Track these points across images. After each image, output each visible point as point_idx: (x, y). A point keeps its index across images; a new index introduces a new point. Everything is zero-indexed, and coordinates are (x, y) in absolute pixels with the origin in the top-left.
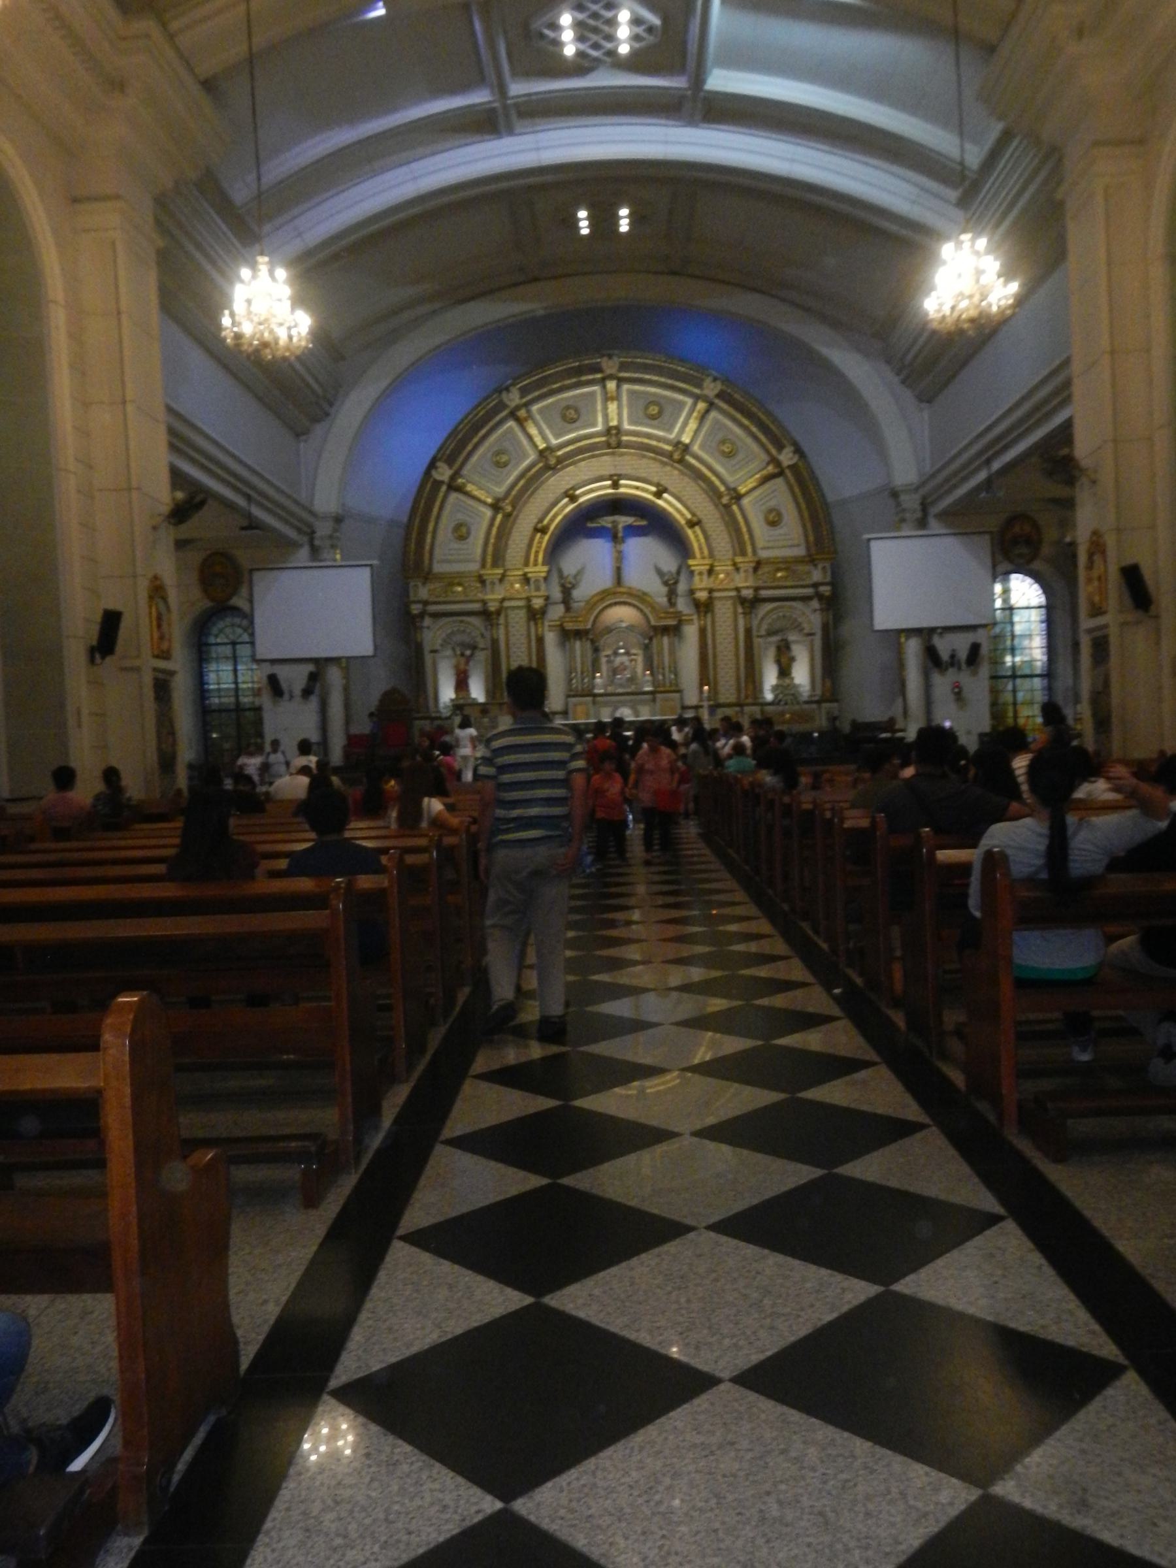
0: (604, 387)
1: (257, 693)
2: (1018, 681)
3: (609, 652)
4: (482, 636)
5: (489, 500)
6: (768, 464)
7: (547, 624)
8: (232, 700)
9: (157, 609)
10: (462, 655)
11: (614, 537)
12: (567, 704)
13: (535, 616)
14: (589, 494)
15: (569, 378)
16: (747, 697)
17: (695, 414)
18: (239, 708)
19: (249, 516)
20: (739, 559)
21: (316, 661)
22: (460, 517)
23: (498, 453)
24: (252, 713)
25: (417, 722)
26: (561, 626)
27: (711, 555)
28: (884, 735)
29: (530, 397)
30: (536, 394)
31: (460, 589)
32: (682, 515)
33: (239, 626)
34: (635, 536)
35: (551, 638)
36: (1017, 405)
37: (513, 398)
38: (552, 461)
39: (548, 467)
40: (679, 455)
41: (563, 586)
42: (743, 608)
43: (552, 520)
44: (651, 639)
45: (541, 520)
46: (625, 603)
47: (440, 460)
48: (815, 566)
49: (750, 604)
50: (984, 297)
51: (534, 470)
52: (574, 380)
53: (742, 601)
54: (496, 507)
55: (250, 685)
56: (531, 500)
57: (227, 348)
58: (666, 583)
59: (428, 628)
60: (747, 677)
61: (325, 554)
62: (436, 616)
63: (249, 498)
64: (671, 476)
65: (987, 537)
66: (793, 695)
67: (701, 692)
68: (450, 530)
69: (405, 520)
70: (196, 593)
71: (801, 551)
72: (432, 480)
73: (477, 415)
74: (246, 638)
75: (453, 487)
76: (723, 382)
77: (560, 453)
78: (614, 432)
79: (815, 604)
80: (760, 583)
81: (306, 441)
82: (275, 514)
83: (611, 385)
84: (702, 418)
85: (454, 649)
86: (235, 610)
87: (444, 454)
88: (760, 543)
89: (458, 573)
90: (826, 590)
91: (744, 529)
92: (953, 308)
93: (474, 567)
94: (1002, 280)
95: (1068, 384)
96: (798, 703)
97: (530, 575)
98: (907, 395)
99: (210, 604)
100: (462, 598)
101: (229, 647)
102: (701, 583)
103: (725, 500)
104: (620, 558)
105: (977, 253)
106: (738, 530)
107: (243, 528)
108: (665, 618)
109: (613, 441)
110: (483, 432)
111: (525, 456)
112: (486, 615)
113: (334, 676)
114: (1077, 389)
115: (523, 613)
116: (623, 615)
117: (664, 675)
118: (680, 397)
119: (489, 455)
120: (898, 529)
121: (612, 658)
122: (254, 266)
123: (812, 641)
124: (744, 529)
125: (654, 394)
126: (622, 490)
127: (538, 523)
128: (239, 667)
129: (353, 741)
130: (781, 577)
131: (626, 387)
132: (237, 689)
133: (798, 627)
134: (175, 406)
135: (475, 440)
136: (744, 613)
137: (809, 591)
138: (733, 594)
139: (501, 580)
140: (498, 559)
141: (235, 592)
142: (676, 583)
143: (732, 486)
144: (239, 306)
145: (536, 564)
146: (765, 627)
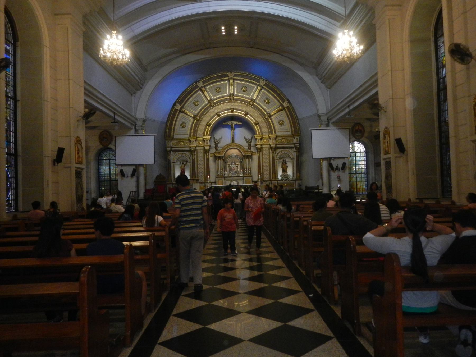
0: (229, 82)
1: (116, 175)
2: (357, 174)
3: (230, 164)
4: (189, 158)
6: (280, 106)
7: (210, 154)
8: (109, 177)
9: (78, 147)
11: (232, 128)
12: (216, 179)
13: (206, 152)
14: (224, 114)
15: (219, 79)
16: (273, 178)
17: (257, 90)
18: (110, 180)
19: (115, 119)
20: (270, 135)
21: (136, 165)
22: (183, 120)
23: (195, 101)
24: (115, 182)
25: (168, 185)
26: (214, 155)
27: (262, 134)
28: (315, 191)
29: (206, 84)
30: (208, 83)
31: (183, 143)
32: (253, 121)
33: (112, 154)
34: (239, 128)
35: (211, 159)
36: (358, 88)
37: (201, 84)
38: (212, 104)
39: (211, 106)
40: (252, 103)
41: (215, 142)
42: (272, 150)
43: (212, 122)
44: (243, 160)
45: (208, 122)
46: (234, 148)
47: (177, 103)
48: (295, 138)
49: (274, 149)
50: (352, 50)
51: (207, 106)
52: (220, 79)
53: (271, 148)
54: (194, 118)
55: (115, 173)
56: (206, 116)
57: (101, 61)
58: (248, 142)
59: (172, 155)
60: (272, 172)
61: (140, 132)
63: (114, 113)
64: (249, 109)
65: (348, 130)
66: (287, 178)
67: (258, 176)
68: (180, 125)
69: (166, 121)
70: (98, 143)
71: (290, 133)
73: (189, 89)
74: (114, 158)
75: (181, 111)
76: (266, 82)
77: (214, 101)
78: (232, 95)
79: (294, 149)
80: (277, 143)
81: (134, 96)
82: (123, 119)
83: (231, 81)
84: (259, 92)
85: (180, 162)
86: (110, 149)
88: (277, 131)
90: (297, 145)
91: (272, 126)
92: (342, 53)
93: (187, 136)
94: (358, 44)
95: (377, 80)
96: (289, 180)
97: (204, 139)
98: (323, 86)
99: (101, 146)
100: (184, 146)
101: (108, 160)
102: (259, 143)
103: (266, 117)
104: (233, 134)
105: (350, 37)
106: (270, 126)
107: (112, 123)
108: (247, 153)
109: (232, 98)
111: (204, 102)
112: (190, 151)
113: (142, 170)
114: (379, 82)
115: (202, 151)
116: (234, 152)
117: (247, 171)
118: (253, 85)
119: (193, 102)
120: (321, 127)
122: (111, 35)
123: (293, 161)
124: (272, 126)
125: (245, 84)
126: (234, 113)
128: (111, 167)
129: (147, 191)
130: (284, 141)
131: (236, 82)
132: (110, 174)
133: (289, 157)
134: (86, 81)
135: (188, 97)
136: (272, 152)
137: (293, 145)
138: (269, 146)
139: (195, 141)
140: (195, 133)
141: (110, 143)
142: (251, 142)
143: (268, 113)
144: (105, 47)
145: (207, 135)
146: (278, 156)
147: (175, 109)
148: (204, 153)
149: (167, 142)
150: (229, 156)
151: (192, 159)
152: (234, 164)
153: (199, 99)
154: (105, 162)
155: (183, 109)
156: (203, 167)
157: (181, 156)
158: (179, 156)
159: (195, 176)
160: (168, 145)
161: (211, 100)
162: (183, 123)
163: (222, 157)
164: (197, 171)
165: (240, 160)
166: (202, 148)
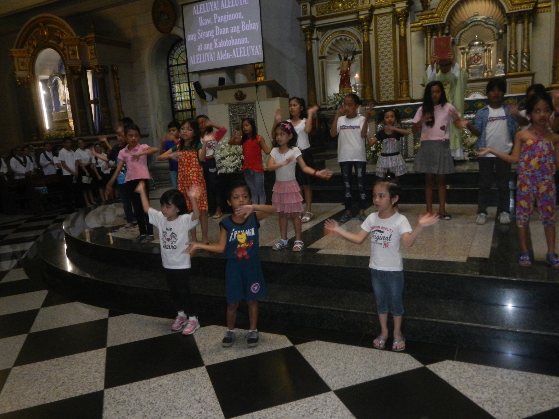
4: (359, 42)
7: (409, 25)
10: (346, 59)
31: (340, 5)
35: (413, 37)
59: (317, 39)
62: (324, 29)
112: (357, 23)
115: (389, 19)
117: (516, 62)
121: (467, 50)
141: (174, 24)
148: (394, 24)
149: (301, 4)
150: (464, 22)
151: (364, 42)
152: (479, 45)
154: (180, 69)
157: (338, 38)
158: (334, 41)
159: (372, 86)
160: (305, 12)
163: (443, 26)
165: (498, 29)
166: (389, 10)
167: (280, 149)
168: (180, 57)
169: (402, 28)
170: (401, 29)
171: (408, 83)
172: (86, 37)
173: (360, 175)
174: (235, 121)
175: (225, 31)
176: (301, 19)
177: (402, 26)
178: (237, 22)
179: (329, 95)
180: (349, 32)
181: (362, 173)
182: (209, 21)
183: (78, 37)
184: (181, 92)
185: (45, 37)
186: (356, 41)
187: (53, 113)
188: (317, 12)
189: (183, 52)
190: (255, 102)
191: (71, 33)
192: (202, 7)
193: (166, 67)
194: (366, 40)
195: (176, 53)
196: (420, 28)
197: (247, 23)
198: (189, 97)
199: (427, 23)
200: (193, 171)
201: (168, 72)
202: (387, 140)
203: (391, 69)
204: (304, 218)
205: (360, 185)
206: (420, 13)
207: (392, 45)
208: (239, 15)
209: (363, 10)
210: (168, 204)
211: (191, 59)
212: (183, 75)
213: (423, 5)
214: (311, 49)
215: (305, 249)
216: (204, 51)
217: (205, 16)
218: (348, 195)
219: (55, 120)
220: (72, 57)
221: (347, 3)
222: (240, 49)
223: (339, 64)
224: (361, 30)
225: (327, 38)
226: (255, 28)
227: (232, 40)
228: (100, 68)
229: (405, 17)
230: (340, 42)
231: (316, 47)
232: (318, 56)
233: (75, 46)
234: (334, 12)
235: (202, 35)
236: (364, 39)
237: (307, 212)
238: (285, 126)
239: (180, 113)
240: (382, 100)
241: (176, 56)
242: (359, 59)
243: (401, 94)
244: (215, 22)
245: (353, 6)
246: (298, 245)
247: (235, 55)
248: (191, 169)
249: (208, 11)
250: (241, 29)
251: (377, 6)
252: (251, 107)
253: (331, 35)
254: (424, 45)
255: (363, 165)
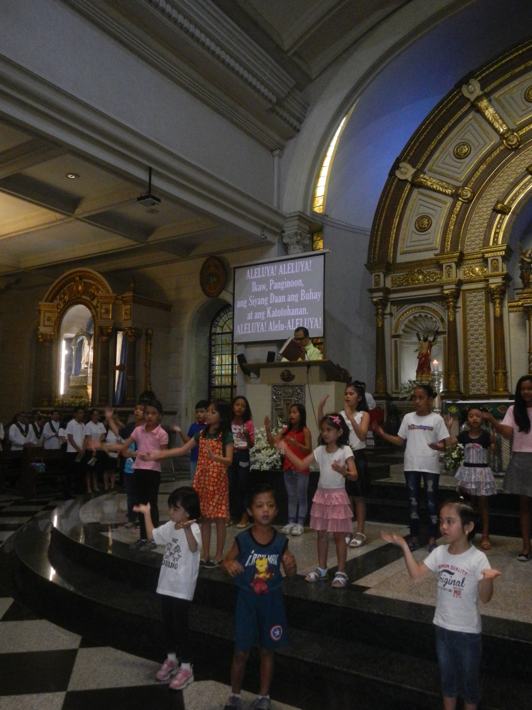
4: (442, 320)
5: (449, 191)
7: (506, 304)
10: (425, 340)
22: (424, 210)
23: (459, 146)
31: (421, 277)
43: (513, 200)
47: (404, 160)
51: (495, 153)
54: (455, 196)
59: (391, 314)
62: (400, 303)
63: (150, 171)
72: (396, 180)
75: (416, 184)
77: (521, 133)
81: (280, 157)
87: (408, 154)
89: (419, 261)
93: (430, 255)
97: (486, 255)
110: (445, 129)
112: (442, 299)
115: (481, 296)
119: (451, 149)
127: (498, 202)
141: (224, 287)
147: (399, 179)
148: (487, 302)
149: (373, 274)
151: (449, 321)
153: (471, 138)
155: (422, 175)
156: (483, 347)
157: (417, 315)
159: (458, 375)
160: (377, 283)
161: (509, 130)
162: (423, 217)
164: (466, 361)
166: (481, 285)
167: (327, 448)
168: (225, 325)
169: (497, 307)
170: (497, 309)
171: (505, 374)
172: (124, 295)
173: (430, 489)
174: (279, 405)
175: (281, 299)
176: (371, 291)
177: (498, 305)
178: (295, 290)
179: (403, 382)
180: (431, 308)
181: (433, 486)
182: (264, 287)
183: (115, 295)
184: (221, 365)
185: (78, 292)
186: (438, 319)
187: (71, 377)
188: (392, 283)
189: (230, 319)
190: (305, 385)
191: (108, 290)
192: (257, 271)
193: (208, 334)
194: (451, 319)
195: (221, 320)
196: (521, 309)
197: (307, 291)
198: (230, 372)
199: (529, 303)
200: (214, 466)
201: (210, 339)
202: (471, 445)
203: (483, 355)
204: (354, 540)
205: (430, 503)
206: (521, 291)
207: (484, 327)
208: (299, 283)
209: (449, 284)
210: (176, 506)
211: (238, 328)
212: (226, 345)
213: (523, 282)
214: (383, 326)
215: (349, 586)
216: (254, 320)
217: (259, 281)
218: (414, 516)
219: (72, 384)
220: (104, 316)
221: (429, 276)
222: (297, 320)
223: (418, 345)
224: (446, 307)
225: (403, 314)
226: (317, 298)
227: (288, 309)
228: (133, 331)
229: (501, 294)
230: (420, 319)
231: (388, 325)
232: (391, 332)
233: (109, 304)
234: (413, 284)
235: (253, 302)
236: (448, 317)
237: (359, 533)
238: (333, 419)
239: (217, 390)
240: (471, 393)
241: (221, 323)
242: (442, 341)
243: (496, 387)
244: (271, 289)
245: (436, 279)
246: (340, 579)
247: (290, 326)
248: (212, 462)
249: (263, 276)
250: (299, 298)
251: (465, 281)
252: (299, 391)
253: (408, 310)
254: (525, 327)
255: (436, 477)
